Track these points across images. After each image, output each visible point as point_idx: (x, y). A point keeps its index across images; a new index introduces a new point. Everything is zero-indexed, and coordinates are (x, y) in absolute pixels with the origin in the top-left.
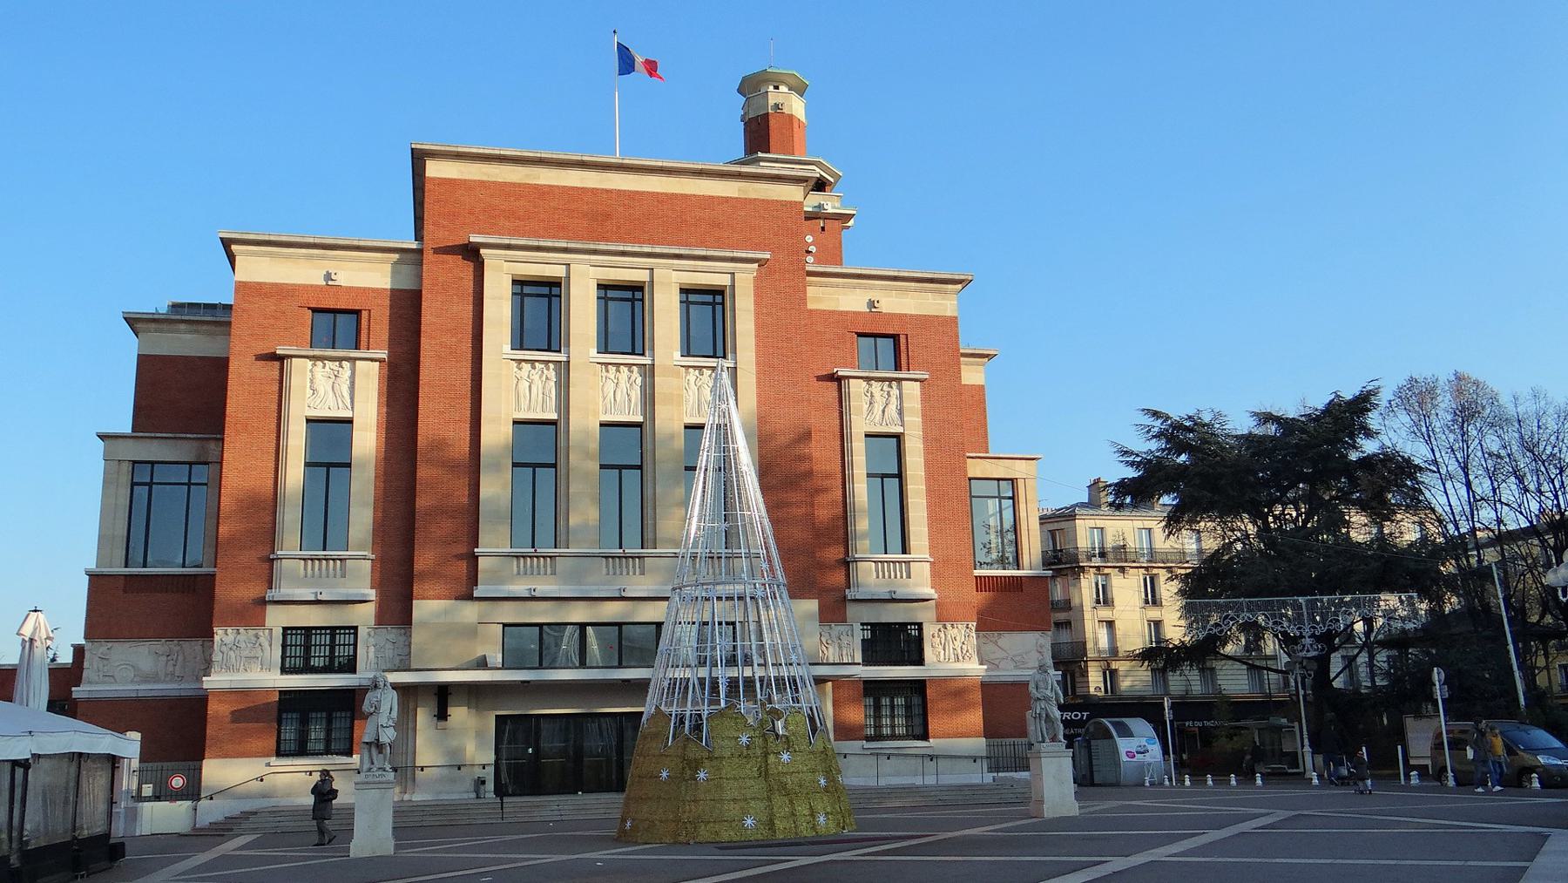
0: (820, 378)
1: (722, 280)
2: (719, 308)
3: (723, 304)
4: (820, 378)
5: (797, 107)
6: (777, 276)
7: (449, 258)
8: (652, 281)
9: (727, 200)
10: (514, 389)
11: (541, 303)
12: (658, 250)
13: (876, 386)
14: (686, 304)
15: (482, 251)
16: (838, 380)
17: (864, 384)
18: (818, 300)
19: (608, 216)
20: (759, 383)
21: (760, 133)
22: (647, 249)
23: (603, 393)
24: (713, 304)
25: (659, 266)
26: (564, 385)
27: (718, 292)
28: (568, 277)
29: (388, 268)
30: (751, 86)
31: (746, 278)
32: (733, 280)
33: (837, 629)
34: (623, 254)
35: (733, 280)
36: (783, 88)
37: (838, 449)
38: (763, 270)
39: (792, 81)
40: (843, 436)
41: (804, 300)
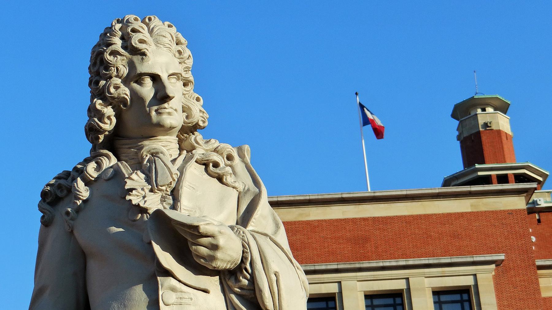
1: (468, 281)
2: (466, 305)
3: (470, 301)
5: (503, 123)
6: (512, 273)
8: (409, 289)
12: (411, 262)
14: (438, 303)
18: (548, 288)
19: (366, 240)
21: (474, 145)
22: (402, 263)
24: (461, 302)
25: (414, 276)
27: (464, 291)
28: (340, 292)
30: (464, 111)
31: (486, 277)
36: (490, 110)
38: (500, 269)
39: (496, 103)
41: (537, 290)
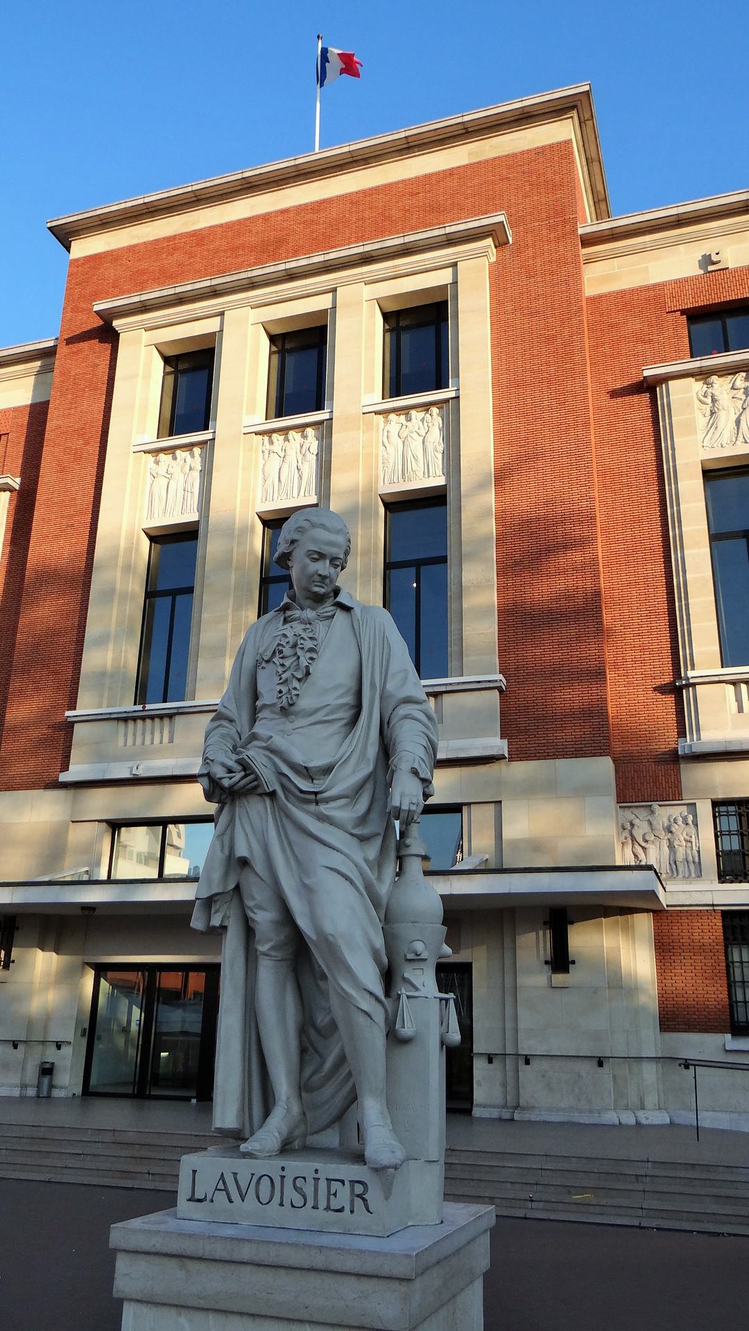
0: (615, 394)
4: (615, 394)
6: (530, 252)
7: (84, 345)
9: (451, 172)
10: (142, 490)
11: (193, 369)
13: (721, 385)
15: (115, 323)
16: (649, 387)
17: (696, 386)
20: (500, 413)
23: (255, 470)
26: (207, 474)
29: (31, 381)
32: (455, 274)
33: (665, 813)
34: (291, 276)
35: (455, 274)
37: (655, 498)
38: (507, 251)
40: (661, 475)
